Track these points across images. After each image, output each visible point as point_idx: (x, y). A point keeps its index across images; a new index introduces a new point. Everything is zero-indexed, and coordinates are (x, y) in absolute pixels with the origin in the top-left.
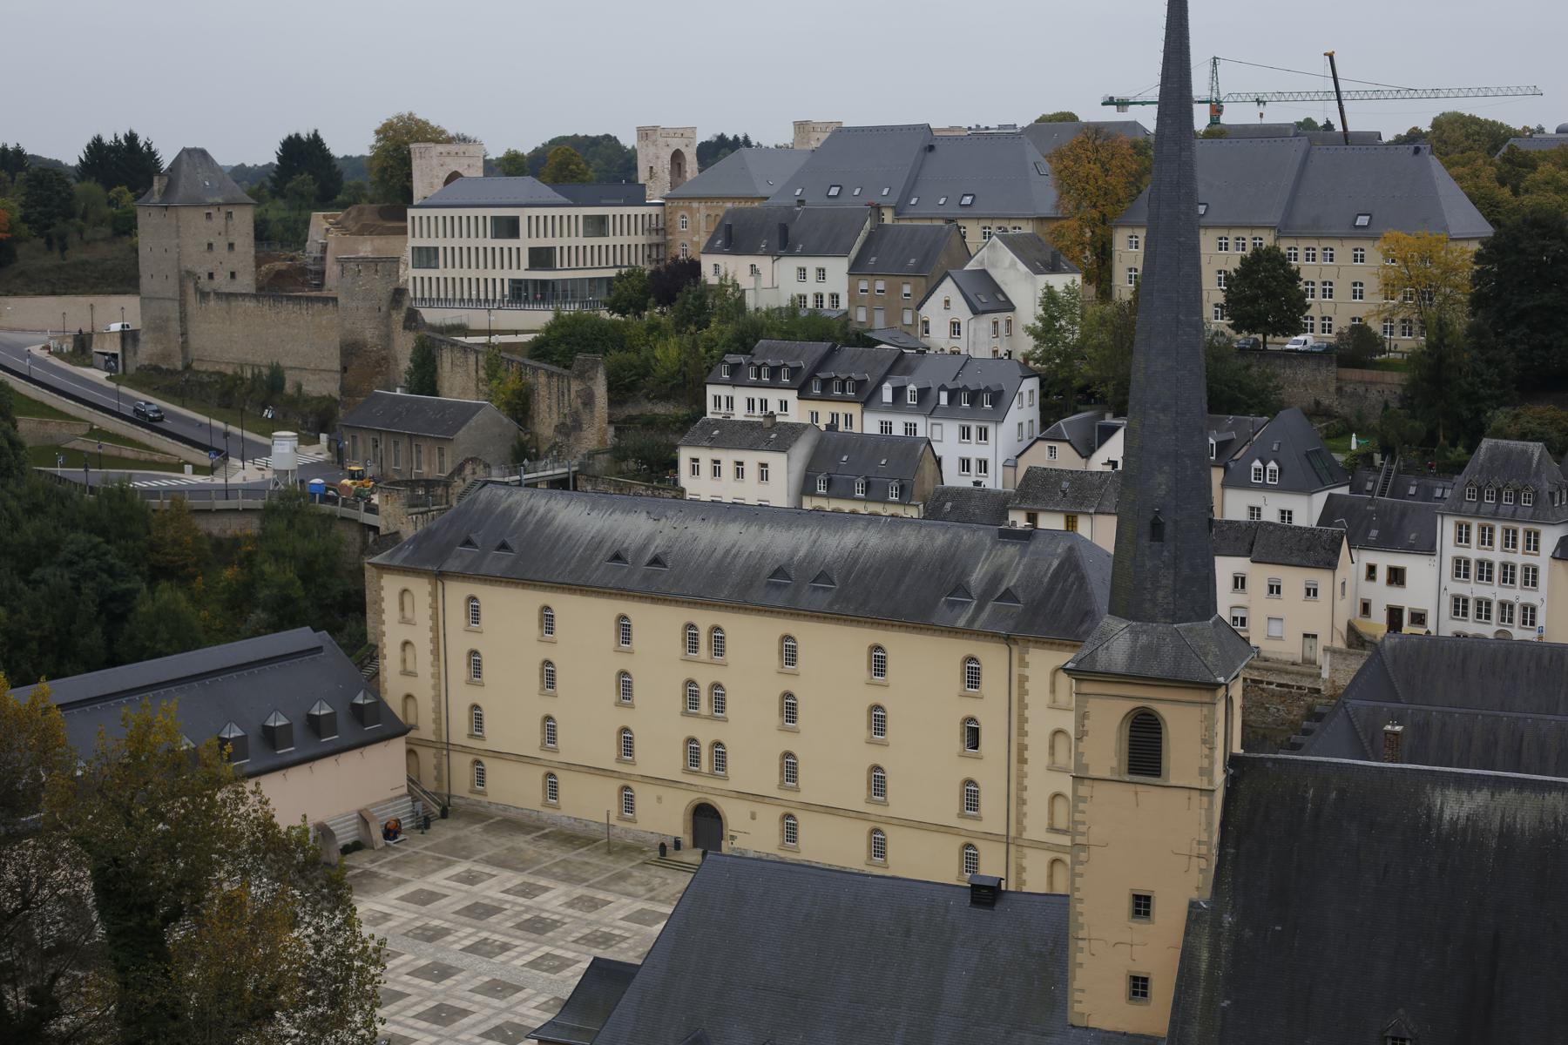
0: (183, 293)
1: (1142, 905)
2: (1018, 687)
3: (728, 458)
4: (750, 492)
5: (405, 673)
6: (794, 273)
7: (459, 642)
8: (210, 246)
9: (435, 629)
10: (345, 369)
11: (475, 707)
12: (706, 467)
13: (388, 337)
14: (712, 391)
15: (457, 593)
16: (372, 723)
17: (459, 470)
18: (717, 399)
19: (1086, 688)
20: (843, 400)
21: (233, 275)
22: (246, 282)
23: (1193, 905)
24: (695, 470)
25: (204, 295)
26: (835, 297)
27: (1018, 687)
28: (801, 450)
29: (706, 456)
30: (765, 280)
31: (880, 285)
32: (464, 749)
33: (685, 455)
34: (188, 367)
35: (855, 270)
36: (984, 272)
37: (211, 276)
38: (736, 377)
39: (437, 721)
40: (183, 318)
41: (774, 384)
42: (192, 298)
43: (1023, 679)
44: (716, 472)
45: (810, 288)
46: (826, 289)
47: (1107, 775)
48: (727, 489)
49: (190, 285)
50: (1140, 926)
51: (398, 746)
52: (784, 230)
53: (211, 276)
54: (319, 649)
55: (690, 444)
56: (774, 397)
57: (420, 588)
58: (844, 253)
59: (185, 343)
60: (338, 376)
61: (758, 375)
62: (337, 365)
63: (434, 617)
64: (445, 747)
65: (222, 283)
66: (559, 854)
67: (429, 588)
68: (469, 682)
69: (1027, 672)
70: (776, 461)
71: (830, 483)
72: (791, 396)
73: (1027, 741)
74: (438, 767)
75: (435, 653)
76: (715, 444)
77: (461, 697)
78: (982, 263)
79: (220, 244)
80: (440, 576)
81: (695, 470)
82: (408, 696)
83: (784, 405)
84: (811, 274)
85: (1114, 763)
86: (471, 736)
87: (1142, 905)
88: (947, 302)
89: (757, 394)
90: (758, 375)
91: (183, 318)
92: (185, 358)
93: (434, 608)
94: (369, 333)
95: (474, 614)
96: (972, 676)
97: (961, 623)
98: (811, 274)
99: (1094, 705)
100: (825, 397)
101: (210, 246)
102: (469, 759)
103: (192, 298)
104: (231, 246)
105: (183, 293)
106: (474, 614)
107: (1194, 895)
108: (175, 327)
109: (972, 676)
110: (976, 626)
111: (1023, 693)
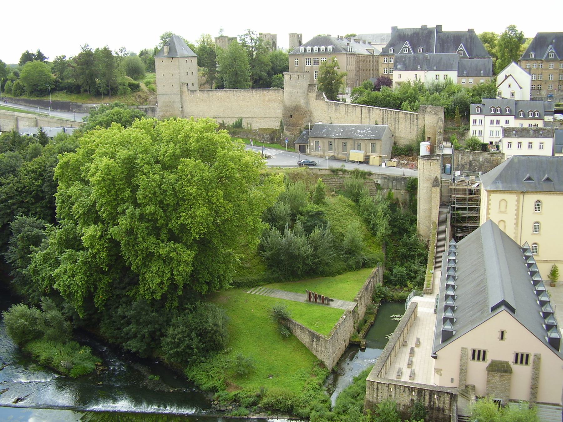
3: (525, 141)
4: (536, 151)
9: (517, 215)
13: (307, 103)
14: (472, 118)
15: (530, 199)
18: (475, 121)
20: (533, 118)
24: (510, 145)
29: (515, 141)
31: (471, 80)
41: (502, 114)
44: (520, 146)
48: (525, 151)
56: (503, 119)
57: (511, 198)
63: (517, 210)
67: (516, 198)
72: (511, 119)
75: (517, 224)
80: (523, 193)
81: (510, 145)
83: (507, 122)
89: (495, 118)
91: (182, 101)
93: (518, 206)
95: (538, 207)
100: (525, 118)
106: (538, 207)
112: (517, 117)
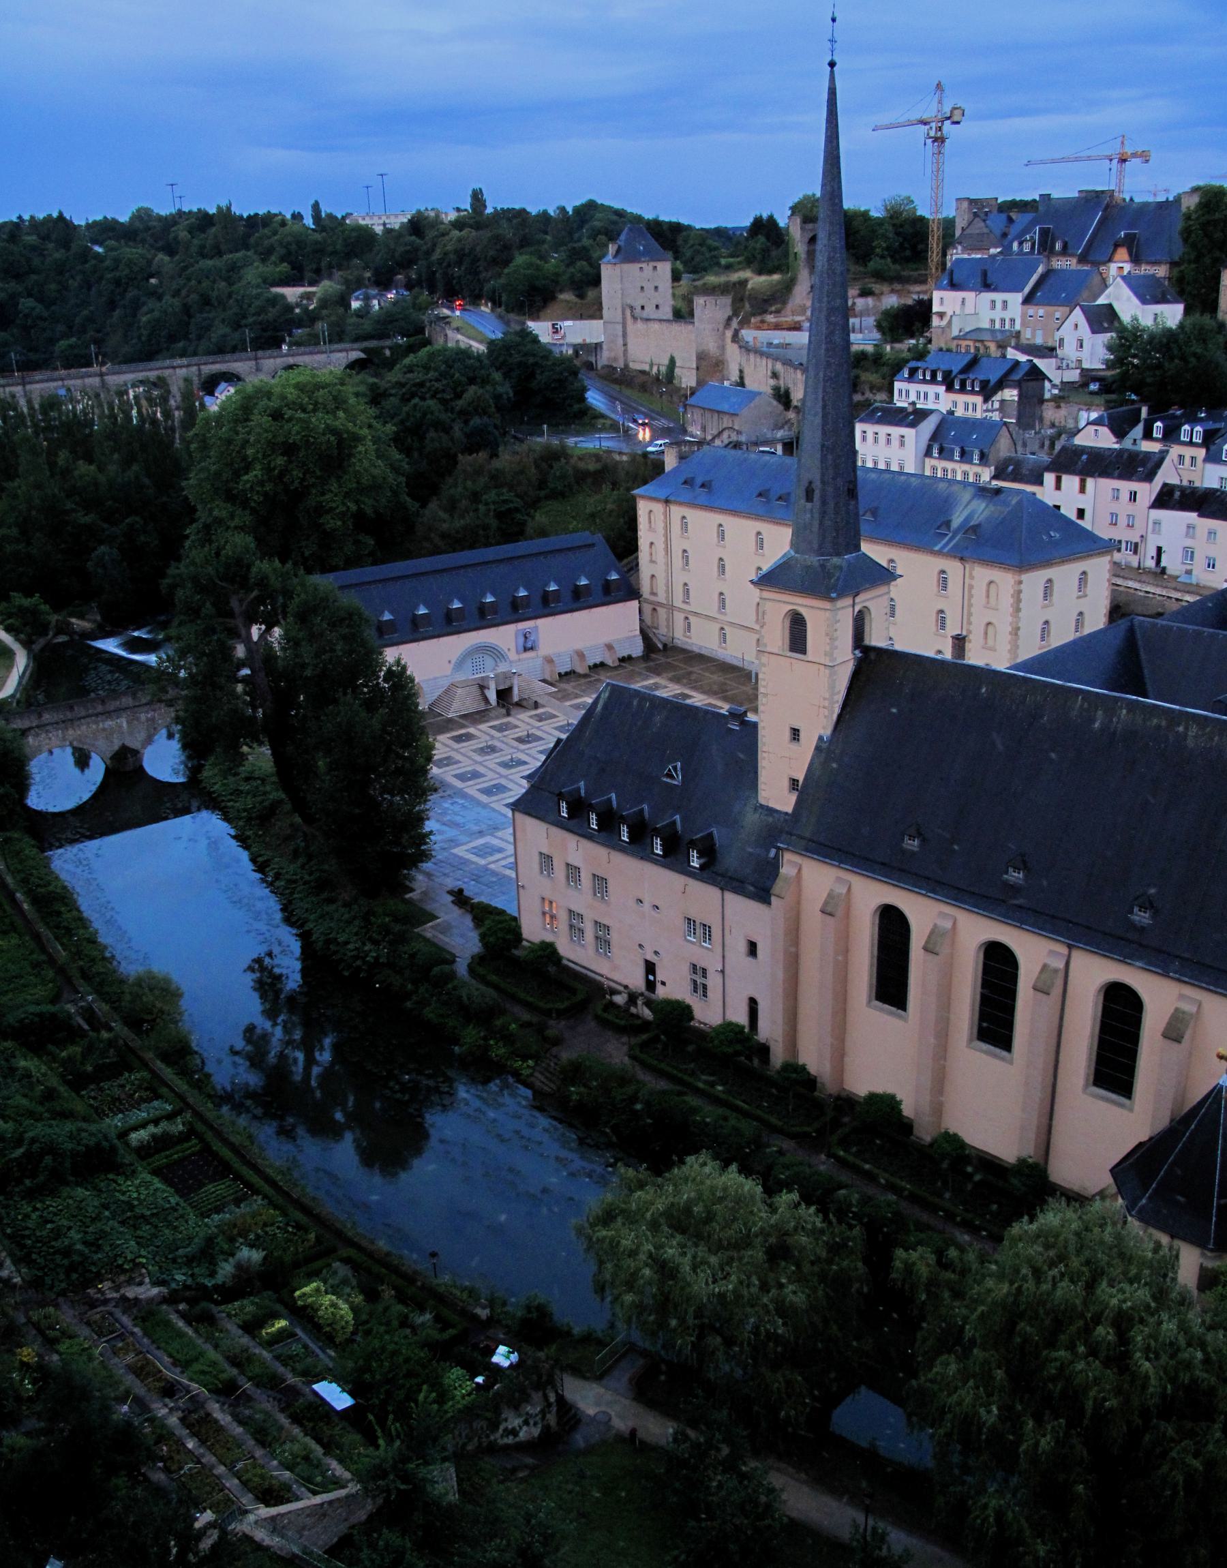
0: (624, 318)
1: (795, 734)
2: (967, 590)
5: (652, 561)
6: (989, 305)
7: (677, 545)
8: (642, 288)
9: (666, 536)
10: (698, 368)
11: (686, 584)
12: (870, 436)
13: (723, 348)
15: (677, 511)
16: (629, 591)
17: (720, 433)
18: (900, 391)
19: (766, 595)
20: (973, 392)
21: (657, 307)
22: (667, 312)
23: (821, 738)
24: (864, 439)
25: (635, 318)
26: (1013, 321)
27: (967, 590)
28: (928, 426)
29: (870, 429)
30: (969, 309)
32: (680, 610)
33: (859, 428)
34: (626, 366)
35: (1027, 301)
36: (1110, 306)
37: (643, 308)
38: (912, 377)
39: (667, 592)
40: (625, 335)
41: (933, 380)
42: (629, 320)
43: (971, 587)
45: (998, 314)
46: (1007, 316)
47: (776, 651)
49: (628, 312)
50: (794, 746)
51: (635, 603)
52: (985, 274)
53: (643, 308)
54: (593, 545)
55: (862, 421)
57: (658, 508)
58: (1018, 289)
59: (625, 351)
60: (694, 372)
61: (924, 375)
62: (694, 366)
64: (671, 608)
65: (650, 311)
66: (716, 677)
68: (684, 569)
69: (973, 583)
70: (909, 433)
71: (941, 451)
73: (971, 628)
74: (667, 620)
76: (880, 421)
77: (679, 578)
78: (1108, 297)
79: (649, 287)
81: (864, 439)
82: (653, 576)
84: (999, 305)
85: (780, 644)
86: (684, 602)
87: (795, 734)
88: (1076, 325)
89: (923, 388)
90: (924, 375)
91: (625, 335)
92: (626, 360)
94: (711, 346)
95: (684, 526)
96: (943, 583)
97: (937, 548)
98: (999, 305)
99: (768, 606)
100: (963, 390)
101: (642, 288)
102: (682, 616)
103: (629, 320)
104: (656, 288)
105: (624, 318)
106: (684, 526)
107: (822, 732)
108: (620, 341)
109: (943, 583)
110: (946, 550)
111: (971, 596)
112: (950, 388)
